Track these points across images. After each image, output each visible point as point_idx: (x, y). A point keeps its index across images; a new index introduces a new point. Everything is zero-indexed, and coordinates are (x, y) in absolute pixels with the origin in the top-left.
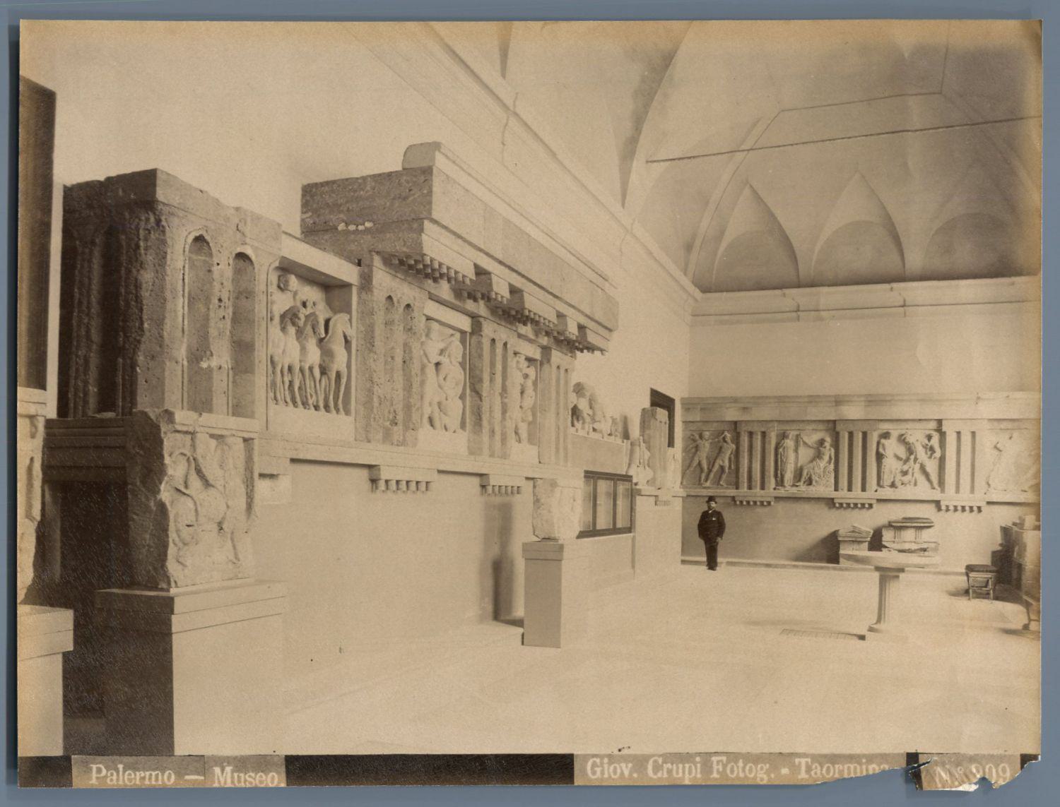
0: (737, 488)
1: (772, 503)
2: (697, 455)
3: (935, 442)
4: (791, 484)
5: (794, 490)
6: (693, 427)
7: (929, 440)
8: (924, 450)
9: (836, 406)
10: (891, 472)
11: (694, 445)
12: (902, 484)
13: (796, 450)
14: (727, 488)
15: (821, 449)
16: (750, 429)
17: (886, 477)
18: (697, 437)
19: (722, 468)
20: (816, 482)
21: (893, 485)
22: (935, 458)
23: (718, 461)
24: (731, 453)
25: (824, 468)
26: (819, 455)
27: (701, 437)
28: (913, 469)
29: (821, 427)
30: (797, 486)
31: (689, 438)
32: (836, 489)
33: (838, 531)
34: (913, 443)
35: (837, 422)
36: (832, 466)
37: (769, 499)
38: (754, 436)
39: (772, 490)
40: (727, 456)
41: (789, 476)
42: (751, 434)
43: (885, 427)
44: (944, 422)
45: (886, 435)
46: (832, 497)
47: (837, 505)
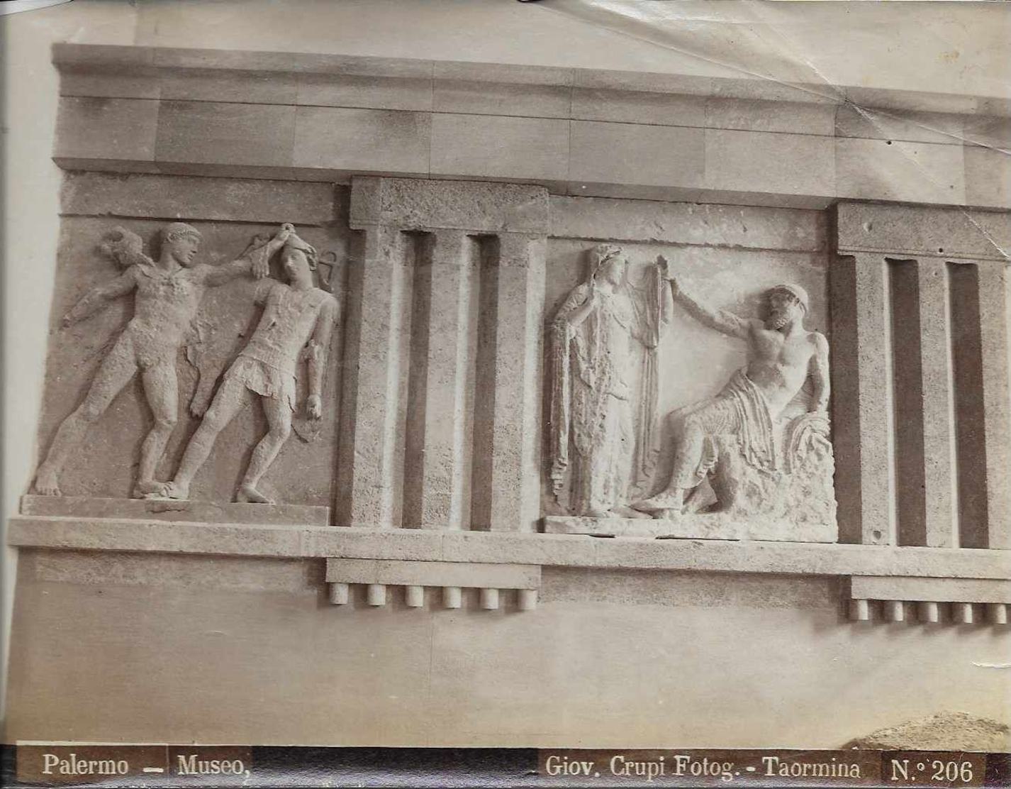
0: (339, 517)
2: (126, 339)
5: (644, 529)
6: (121, 198)
9: (838, 135)
11: (118, 284)
14: (281, 515)
15: (768, 334)
16: (419, 219)
18: (136, 244)
19: (260, 405)
23: (239, 369)
24: (314, 335)
27: (157, 249)
29: (761, 233)
30: (654, 514)
31: (98, 251)
32: (850, 533)
35: (842, 210)
36: (821, 420)
38: (438, 254)
47: (864, 612)
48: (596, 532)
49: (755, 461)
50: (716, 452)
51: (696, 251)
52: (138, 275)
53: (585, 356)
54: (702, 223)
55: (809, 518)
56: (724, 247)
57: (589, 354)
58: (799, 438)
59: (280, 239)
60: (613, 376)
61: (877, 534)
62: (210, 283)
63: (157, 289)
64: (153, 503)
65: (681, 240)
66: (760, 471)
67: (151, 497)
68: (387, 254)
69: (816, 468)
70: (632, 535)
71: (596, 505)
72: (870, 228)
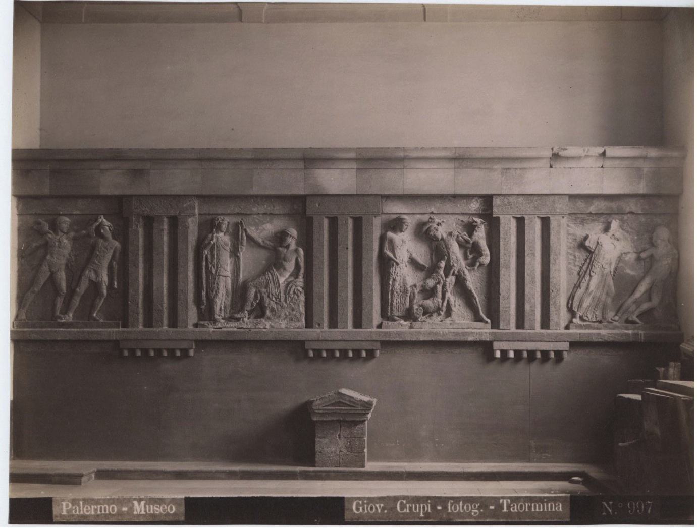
1: (192, 353)
3: (480, 235)
4: (227, 316)
7: (471, 234)
8: (462, 251)
10: (406, 291)
12: (424, 314)
13: (235, 253)
17: (396, 300)
18: (47, 227)
19: (95, 286)
20: (272, 310)
21: (409, 315)
22: (481, 265)
24: (113, 257)
25: (287, 285)
26: (276, 262)
27: (54, 227)
28: (444, 286)
29: (278, 209)
30: (238, 320)
32: (309, 324)
33: (312, 402)
34: (442, 239)
35: (308, 199)
36: (300, 281)
37: (184, 345)
38: (155, 225)
39: (190, 327)
40: (105, 263)
41: (222, 300)
42: (150, 222)
43: (395, 209)
44: (497, 201)
45: (396, 225)
46: (300, 338)
48: (215, 327)
49: (274, 299)
50: (259, 296)
51: (255, 216)
52: (48, 238)
53: (211, 262)
54: (257, 205)
55: (293, 319)
56: (265, 214)
57: (212, 261)
58: (290, 289)
59: (98, 222)
60: (221, 269)
61: (319, 325)
62: (74, 239)
63: (55, 244)
64: (59, 322)
65: (248, 213)
66: (276, 302)
67: (59, 321)
68: (137, 226)
69: (297, 300)
70: (227, 328)
71: (217, 317)
72: (319, 205)
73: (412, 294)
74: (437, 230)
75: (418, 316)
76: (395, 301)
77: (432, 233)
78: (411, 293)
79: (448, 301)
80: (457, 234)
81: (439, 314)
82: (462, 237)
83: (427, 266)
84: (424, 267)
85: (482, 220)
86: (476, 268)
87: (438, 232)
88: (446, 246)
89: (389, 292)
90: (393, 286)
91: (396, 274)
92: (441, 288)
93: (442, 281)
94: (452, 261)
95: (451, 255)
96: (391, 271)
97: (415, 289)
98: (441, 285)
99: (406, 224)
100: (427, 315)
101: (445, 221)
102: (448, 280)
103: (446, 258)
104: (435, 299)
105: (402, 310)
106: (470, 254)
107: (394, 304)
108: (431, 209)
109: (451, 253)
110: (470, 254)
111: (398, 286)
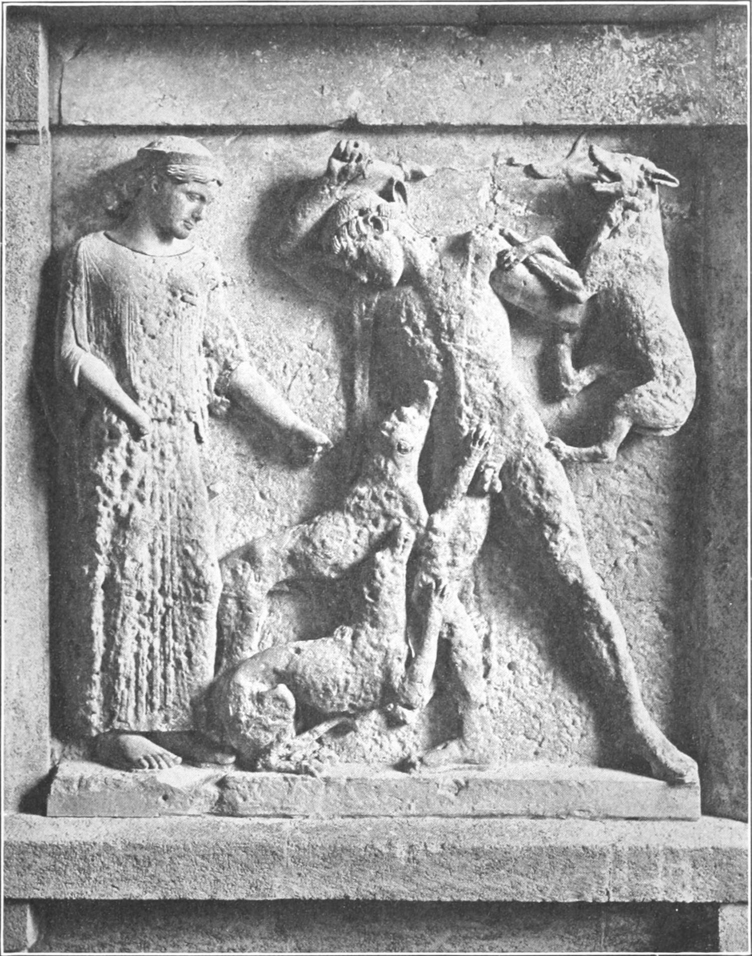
8: (530, 349)
34: (411, 275)
73: (231, 604)
74: (377, 224)
75: (266, 738)
76: (129, 646)
77: (347, 243)
78: (224, 598)
79: (446, 647)
80: (505, 245)
81: (393, 722)
82: (526, 263)
83: (321, 437)
84: (307, 444)
85: (651, 166)
86: (611, 449)
87: (386, 235)
88: (433, 322)
89: (91, 594)
90: (118, 556)
91: (133, 485)
92: (402, 570)
93: (408, 533)
94: (468, 409)
95: (461, 375)
96: (102, 471)
97: (248, 574)
98: (404, 554)
99: (193, 187)
100: (323, 729)
101: (427, 170)
102: (445, 522)
103: (433, 390)
104: (368, 633)
105: (171, 697)
106: (578, 365)
107: (126, 663)
108: (342, 98)
109: (461, 361)
110: (578, 365)
111: (143, 554)
